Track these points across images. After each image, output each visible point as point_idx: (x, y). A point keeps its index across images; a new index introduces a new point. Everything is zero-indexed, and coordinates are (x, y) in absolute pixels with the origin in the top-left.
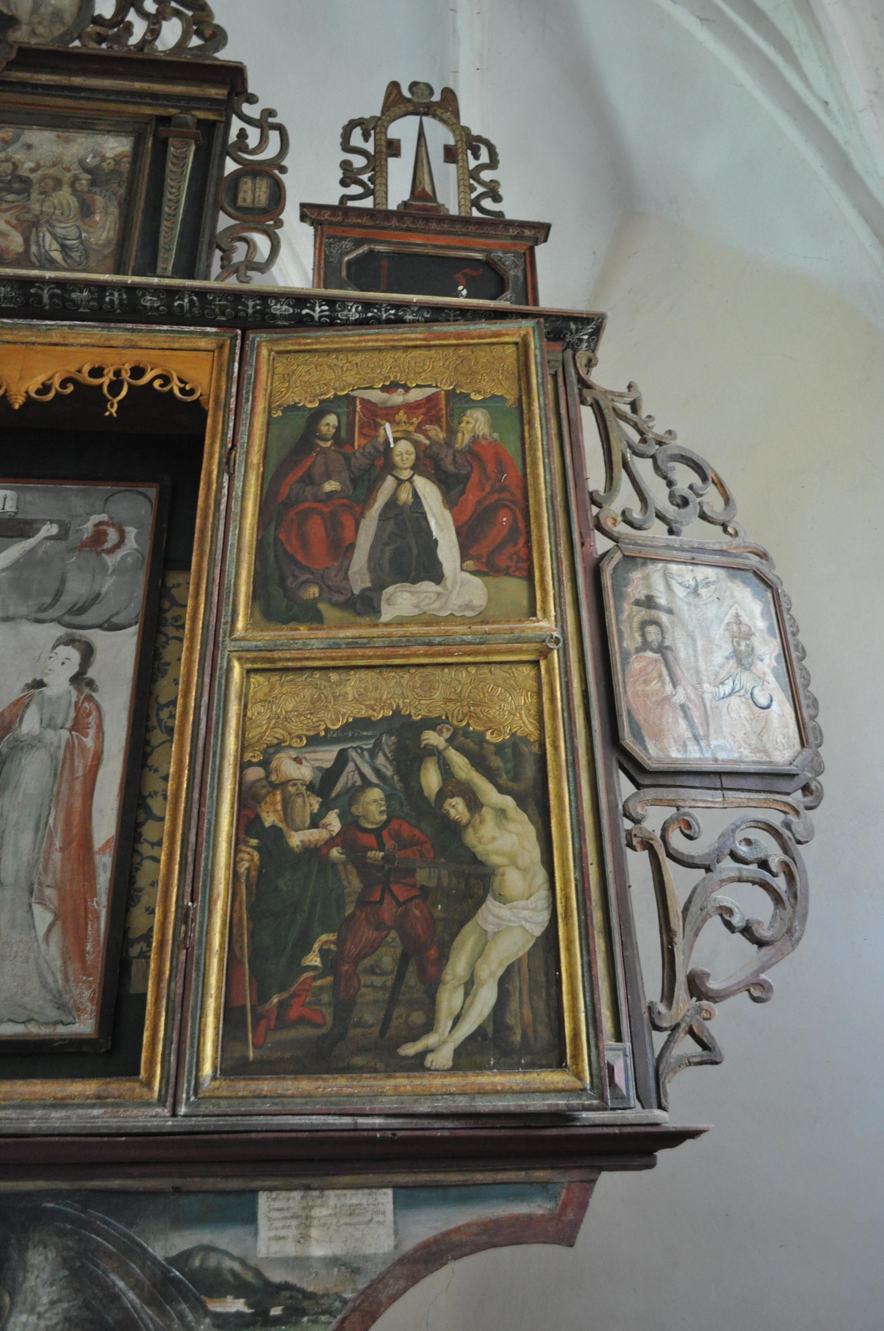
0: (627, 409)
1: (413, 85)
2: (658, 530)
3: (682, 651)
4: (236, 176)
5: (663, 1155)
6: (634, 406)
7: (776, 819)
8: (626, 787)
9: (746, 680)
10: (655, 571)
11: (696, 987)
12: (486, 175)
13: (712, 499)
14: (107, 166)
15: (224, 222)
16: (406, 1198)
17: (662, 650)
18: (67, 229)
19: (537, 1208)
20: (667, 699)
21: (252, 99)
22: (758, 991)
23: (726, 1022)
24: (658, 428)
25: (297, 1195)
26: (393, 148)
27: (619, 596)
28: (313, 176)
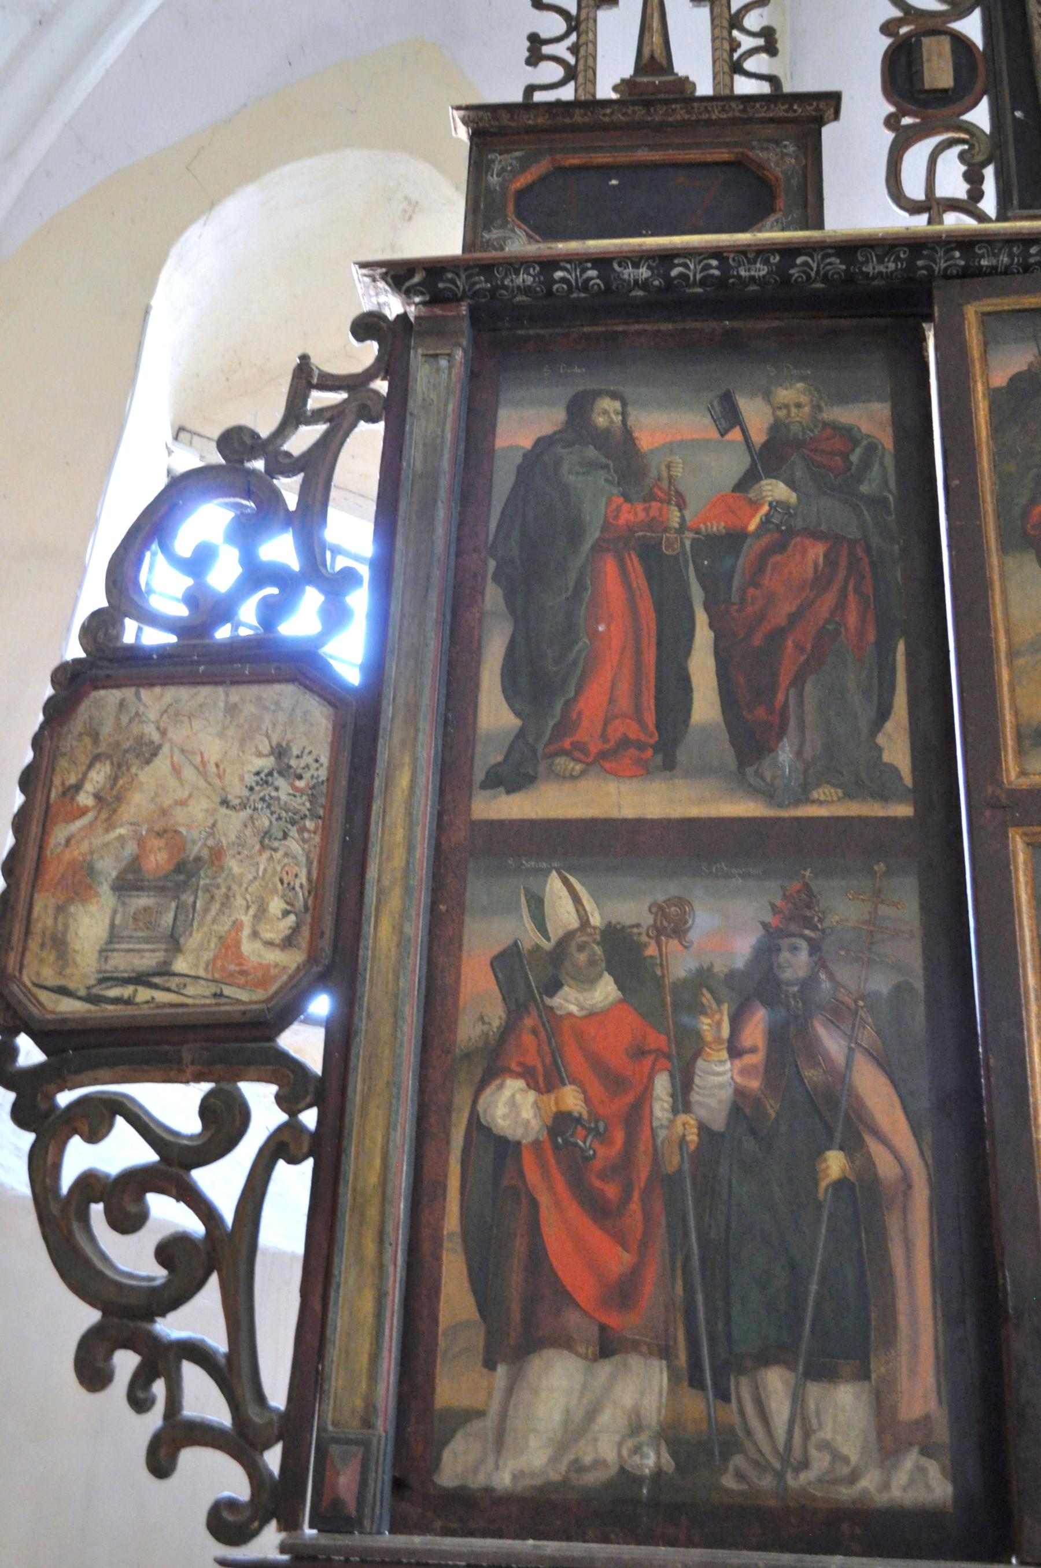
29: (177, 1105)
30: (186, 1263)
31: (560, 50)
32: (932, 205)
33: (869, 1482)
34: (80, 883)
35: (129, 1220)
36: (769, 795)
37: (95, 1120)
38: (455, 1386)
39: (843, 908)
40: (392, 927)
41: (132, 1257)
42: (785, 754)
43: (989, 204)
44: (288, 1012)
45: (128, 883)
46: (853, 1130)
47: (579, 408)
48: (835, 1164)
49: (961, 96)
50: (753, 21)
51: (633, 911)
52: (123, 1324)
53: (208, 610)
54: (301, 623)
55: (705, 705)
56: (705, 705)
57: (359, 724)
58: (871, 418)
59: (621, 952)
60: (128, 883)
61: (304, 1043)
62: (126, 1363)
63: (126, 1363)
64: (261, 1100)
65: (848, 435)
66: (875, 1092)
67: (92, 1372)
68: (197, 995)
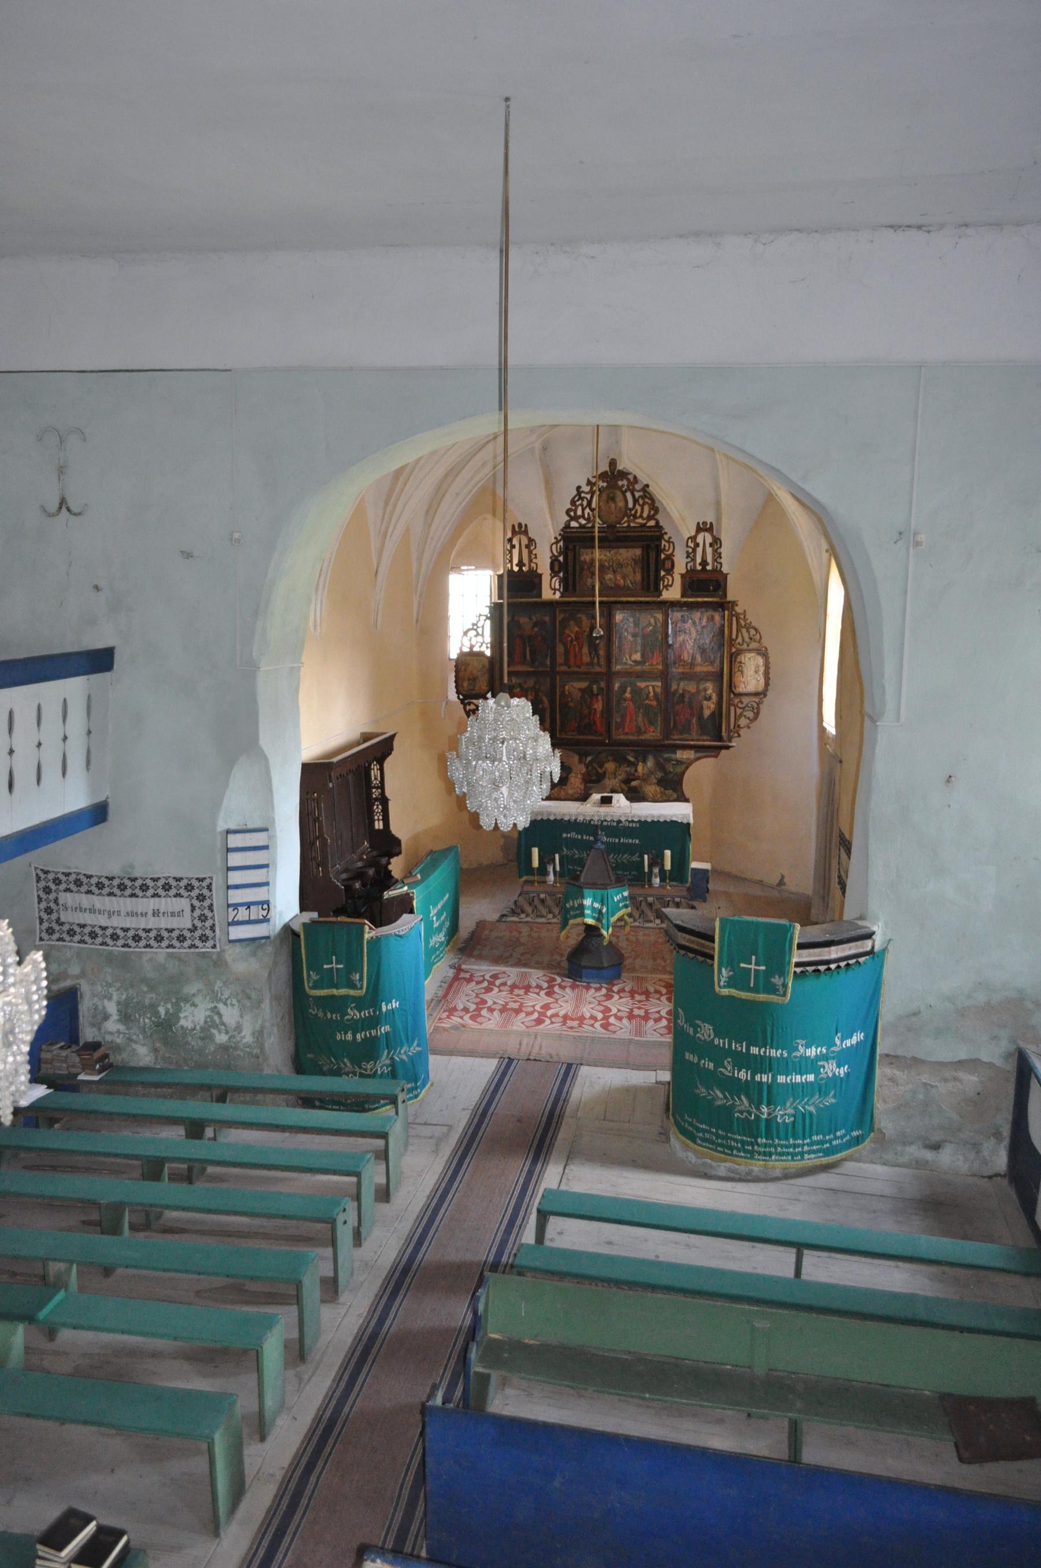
3: (745, 670)
11: (739, 726)
15: (663, 573)
16: (696, 752)
22: (749, 727)
23: (741, 732)
26: (697, 545)
28: (681, 565)
32: (555, 589)
34: (464, 680)
37: (469, 703)
45: (469, 679)
46: (542, 703)
49: (559, 572)
53: (472, 647)
54: (483, 649)
55: (528, 657)
56: (528, 657)
57: (491, 660)
58: (547, 619)
59: (520, 685)
66: (545, 699)
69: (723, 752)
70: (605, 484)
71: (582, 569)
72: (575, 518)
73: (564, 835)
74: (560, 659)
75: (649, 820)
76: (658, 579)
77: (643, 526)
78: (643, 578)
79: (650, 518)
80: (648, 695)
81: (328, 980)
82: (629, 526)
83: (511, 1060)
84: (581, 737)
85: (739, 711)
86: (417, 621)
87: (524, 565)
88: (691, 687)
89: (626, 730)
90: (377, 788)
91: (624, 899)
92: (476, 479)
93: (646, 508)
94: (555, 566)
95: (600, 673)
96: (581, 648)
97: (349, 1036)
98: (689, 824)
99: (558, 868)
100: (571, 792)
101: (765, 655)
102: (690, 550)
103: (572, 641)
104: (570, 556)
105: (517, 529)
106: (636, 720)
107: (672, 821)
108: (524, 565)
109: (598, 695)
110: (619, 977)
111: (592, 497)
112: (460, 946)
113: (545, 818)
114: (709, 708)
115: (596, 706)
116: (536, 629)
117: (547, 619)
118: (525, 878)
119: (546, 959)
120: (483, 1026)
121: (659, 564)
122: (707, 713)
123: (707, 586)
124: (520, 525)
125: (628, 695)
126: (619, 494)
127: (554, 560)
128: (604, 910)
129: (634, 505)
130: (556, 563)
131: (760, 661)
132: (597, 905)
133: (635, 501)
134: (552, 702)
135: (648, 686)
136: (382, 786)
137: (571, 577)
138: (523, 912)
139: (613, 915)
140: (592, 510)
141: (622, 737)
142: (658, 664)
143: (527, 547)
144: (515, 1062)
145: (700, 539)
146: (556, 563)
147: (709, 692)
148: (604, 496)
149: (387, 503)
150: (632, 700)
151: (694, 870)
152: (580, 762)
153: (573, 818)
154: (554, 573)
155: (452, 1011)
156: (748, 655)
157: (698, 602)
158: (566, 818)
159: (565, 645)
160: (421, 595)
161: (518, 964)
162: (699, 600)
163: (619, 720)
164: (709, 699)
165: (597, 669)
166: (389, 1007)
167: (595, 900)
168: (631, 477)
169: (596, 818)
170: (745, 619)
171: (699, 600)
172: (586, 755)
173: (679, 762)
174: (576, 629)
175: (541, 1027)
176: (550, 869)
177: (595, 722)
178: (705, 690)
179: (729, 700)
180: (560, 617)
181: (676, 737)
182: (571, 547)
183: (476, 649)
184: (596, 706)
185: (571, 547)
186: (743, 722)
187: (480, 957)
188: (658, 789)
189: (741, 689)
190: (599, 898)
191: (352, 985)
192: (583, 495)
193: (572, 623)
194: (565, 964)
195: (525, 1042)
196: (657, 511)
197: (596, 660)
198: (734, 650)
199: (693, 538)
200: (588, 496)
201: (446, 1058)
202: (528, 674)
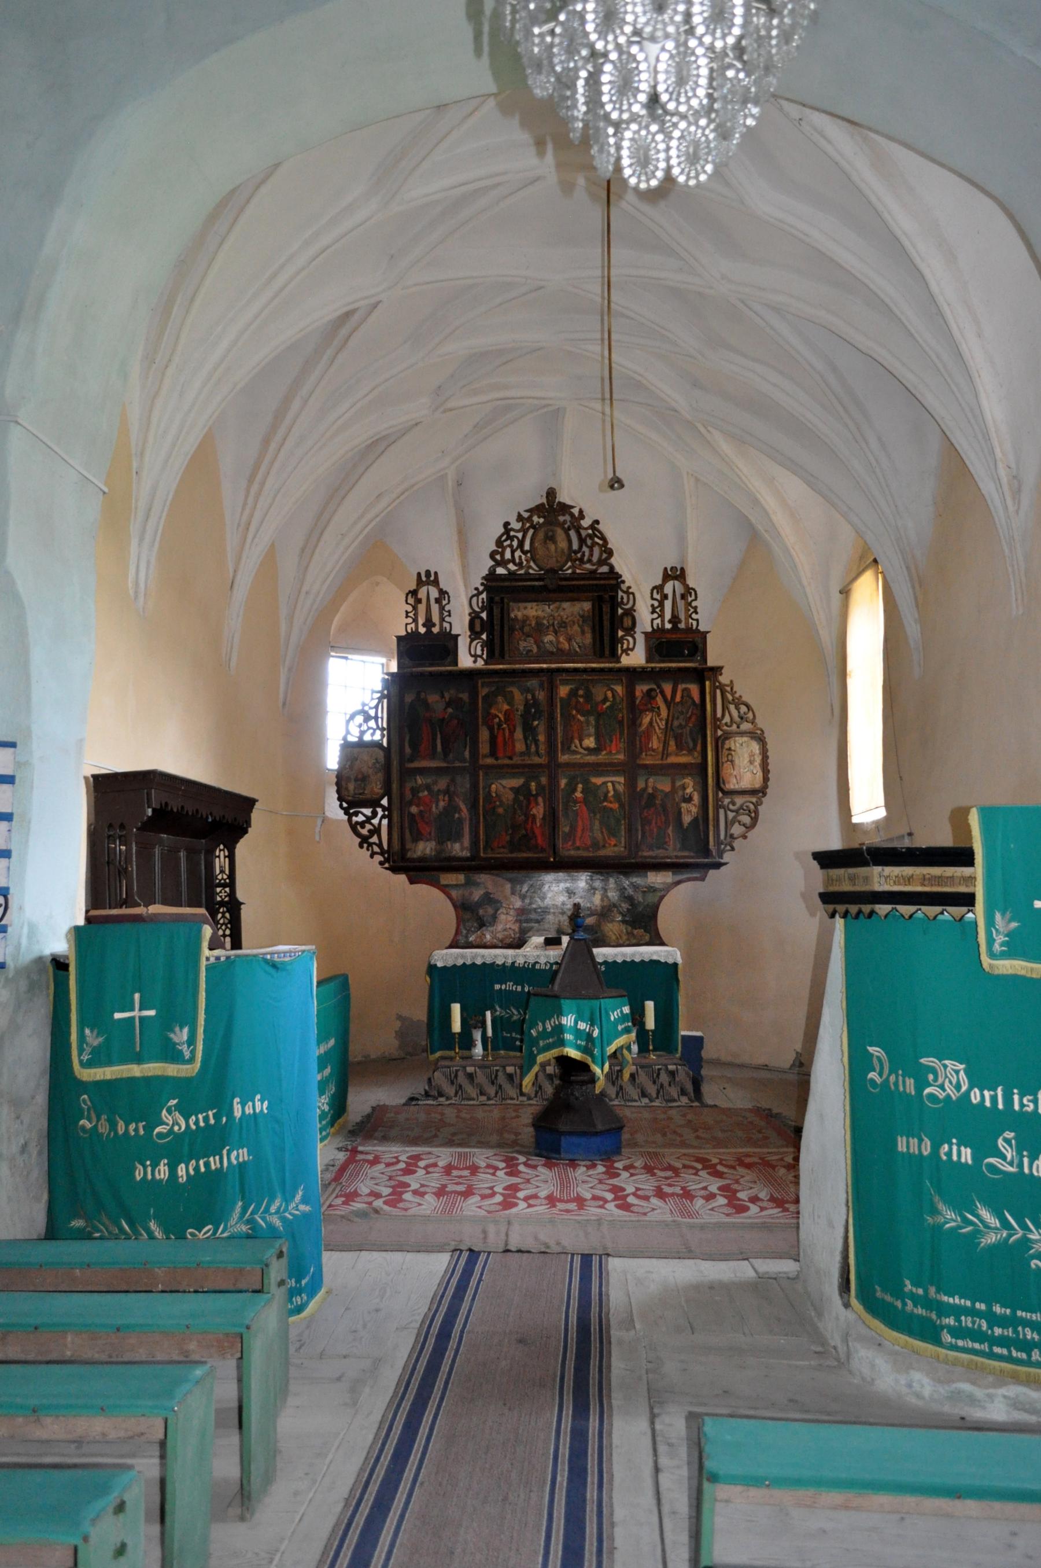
0: (728, 689)
1: (672, 568)
2: (735, 726)
3: (737, 762)
4: (623, 615)
5: (723, 868)
6: (732, 689)
7: (754, 800)
8: (720, 795)
9: (752, 767)
10: (732, 741)
11: (732, 836)
12: (694, 604)
13: (750, 715)
14: (586, 614)
15: (620, 633)
17: (732, 761)
18: (578, 640)
19: (698, 875)
20: (731, 775)
21: (623, 582)
22: (745, 837)
23: (735, 844)
24: (737, 695)
25: (654, 873)
26: (666, 597)
27: (722, 747)
29: (368, 812)
30: (372, 833)
31: (411, 615)
33: (460, 854)
35: (363, 827)
36: (448, 762)
37: (356, 814)
38: (409, 845)
39: (459, 779)
40: (395, 786)
41: (364, 832)
42: (451, 755)
43: (485, 656)
44: (382, 798)
45: (356, 780)
46: (460, 811)
47: (418, 693)
48: (457, 815)
50: (447, 608)
51: (429, 781)
52: (364, 841)
53: (362, 733)
58: (465, 696)
60: (356, 780)
61: (385, 802)
62: (365, 845)
63: (365, 845)
64: (379, 810)
65: (461, 699)
66: (463, 806)
67: (361, 846)
68: (369, 796)
69: (712, 872)
70: (541, 520)
71: (512, 630)
72: (503, 563)
73: (497, 987)
74: (484, 748)
75: (619, 961)
76: (615, 641)
77: (596, 570)
78: (594, 639)
79: (602, 562)
80: (606, 798)
81: (121, 1045)
82: (574, 573)
83: (474, 1254)
84: (514, 855)
85: (731, 815)
86: (284, 704)
87: (434, 625)
88: (664, 785)
89: (578, 844)
90: (224, 886)
91: (623, 1018)
92: (369, 516)
93: (596, 550)
94: (475, 627)
95: (540, 766)
96: (512, 732)
97: (163, 1172)
98: (675, 965)
99: (490, 1033)
100: (500, 936)
101: (761, 740)
102: (656, 604)
103: (500, 725)
104: (496, 611)
105: (424, 579)
106: (592, 830)
107: (651, 961)
108: (434, 625)
109: (537, 795)
110: (617, 1151)
111: (524, 537)
112: (350, 1128)
113: (469, 962)
114: (689, 812)
115: (534, 811)
116: (450, 710)
117: (465, 696)
118: (438, 1054)
119: (494, 1138)
120: (410, 1212)
121: (616, 622)
122: (687, 819)
123: (681, 647)
124: (428, 573)
125: (578, 795)
126: (560, 534)
127: (474, 617)
128: (596, 1033)
129: (581, 547)
130: (478, 622)
131: (755, 747)
132: (582, 1026)
133: (582, 541)
134: (474, 806)
135: (605, 783)
136: (231, 882)
137: (497, 641)
138: (441, 1095)
139: (609, 1043)
140: (525, 553)
141: (572, 853)
142: (618, 752)
143: (437, 601)
144: (482, 1257)
145: (668, 589)
146: (478, 622)
147: (689, 791)
148: (541, 535)
149: (251, 480)
150: (585, 801)
151: (683, 1037)
152: (513, 893)
153: (510, 961)
154: (474, 634)
155: (351, 1197)
156: (740, 740)
157: (670, 669)
158: (500, 962)
159: (491, 729)
160: (290, 670)
161: (450, 1143)
162: (674, 665)
163: (567, 829)
164: (689, 800)
165: (537, 760)
166: (249, 1110)
167: (580, 1018)
168: (576, 511)
169: (543, 960)
170: (733, 693)
171: (674, 665)
172: (522, 883)
173: (652, 890)
174: (506, 707)
175: (514, 1210)
176: (477, 1035)
177: (534, 833)
178: (684, 787)
179: (717, 800)
180: (484, 691)
181: (645, 854)
182: (497, 599)
183: (367, 737)
184: (534, 811)
185: (497, 599)
186: (737, 830)
187: (385, 1139)
188: (623, 927)
189: (732, 785)
190: (587, 1014)
191: (172, 1054)
192: (512, 533)
193: (500, 699)
194: (528, 1133)
195: (491, 1229)
196: (610, 553)
197: (533, 748)
198: (720, 733)
199: (659, 588)
200: (520, 535)
201: (348, 1257)
202: (439, 771)
